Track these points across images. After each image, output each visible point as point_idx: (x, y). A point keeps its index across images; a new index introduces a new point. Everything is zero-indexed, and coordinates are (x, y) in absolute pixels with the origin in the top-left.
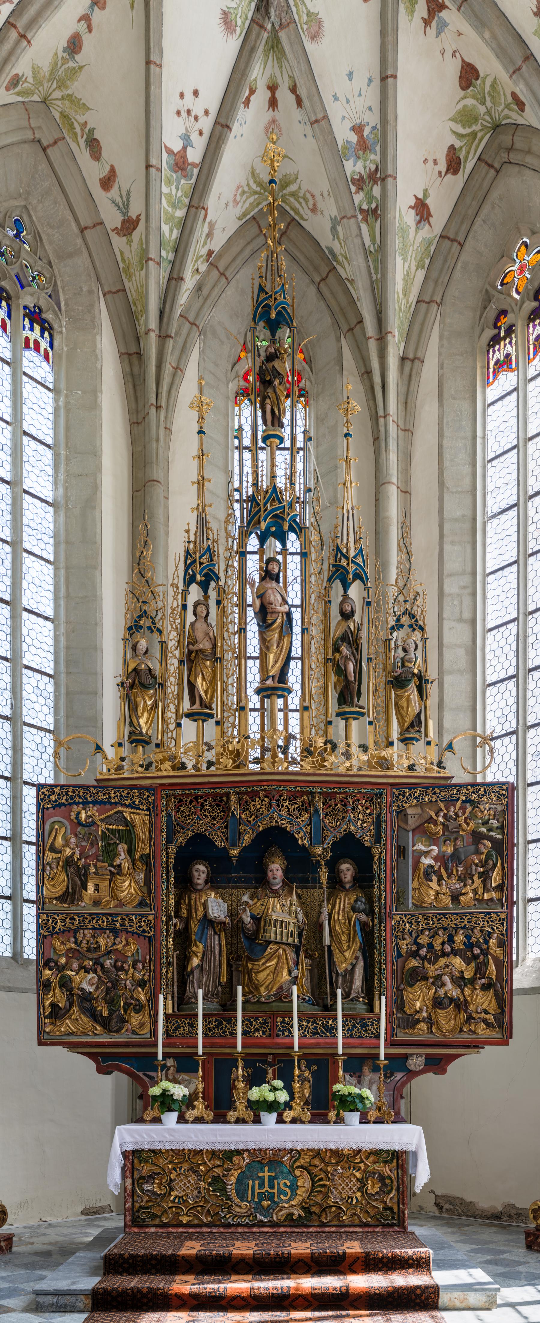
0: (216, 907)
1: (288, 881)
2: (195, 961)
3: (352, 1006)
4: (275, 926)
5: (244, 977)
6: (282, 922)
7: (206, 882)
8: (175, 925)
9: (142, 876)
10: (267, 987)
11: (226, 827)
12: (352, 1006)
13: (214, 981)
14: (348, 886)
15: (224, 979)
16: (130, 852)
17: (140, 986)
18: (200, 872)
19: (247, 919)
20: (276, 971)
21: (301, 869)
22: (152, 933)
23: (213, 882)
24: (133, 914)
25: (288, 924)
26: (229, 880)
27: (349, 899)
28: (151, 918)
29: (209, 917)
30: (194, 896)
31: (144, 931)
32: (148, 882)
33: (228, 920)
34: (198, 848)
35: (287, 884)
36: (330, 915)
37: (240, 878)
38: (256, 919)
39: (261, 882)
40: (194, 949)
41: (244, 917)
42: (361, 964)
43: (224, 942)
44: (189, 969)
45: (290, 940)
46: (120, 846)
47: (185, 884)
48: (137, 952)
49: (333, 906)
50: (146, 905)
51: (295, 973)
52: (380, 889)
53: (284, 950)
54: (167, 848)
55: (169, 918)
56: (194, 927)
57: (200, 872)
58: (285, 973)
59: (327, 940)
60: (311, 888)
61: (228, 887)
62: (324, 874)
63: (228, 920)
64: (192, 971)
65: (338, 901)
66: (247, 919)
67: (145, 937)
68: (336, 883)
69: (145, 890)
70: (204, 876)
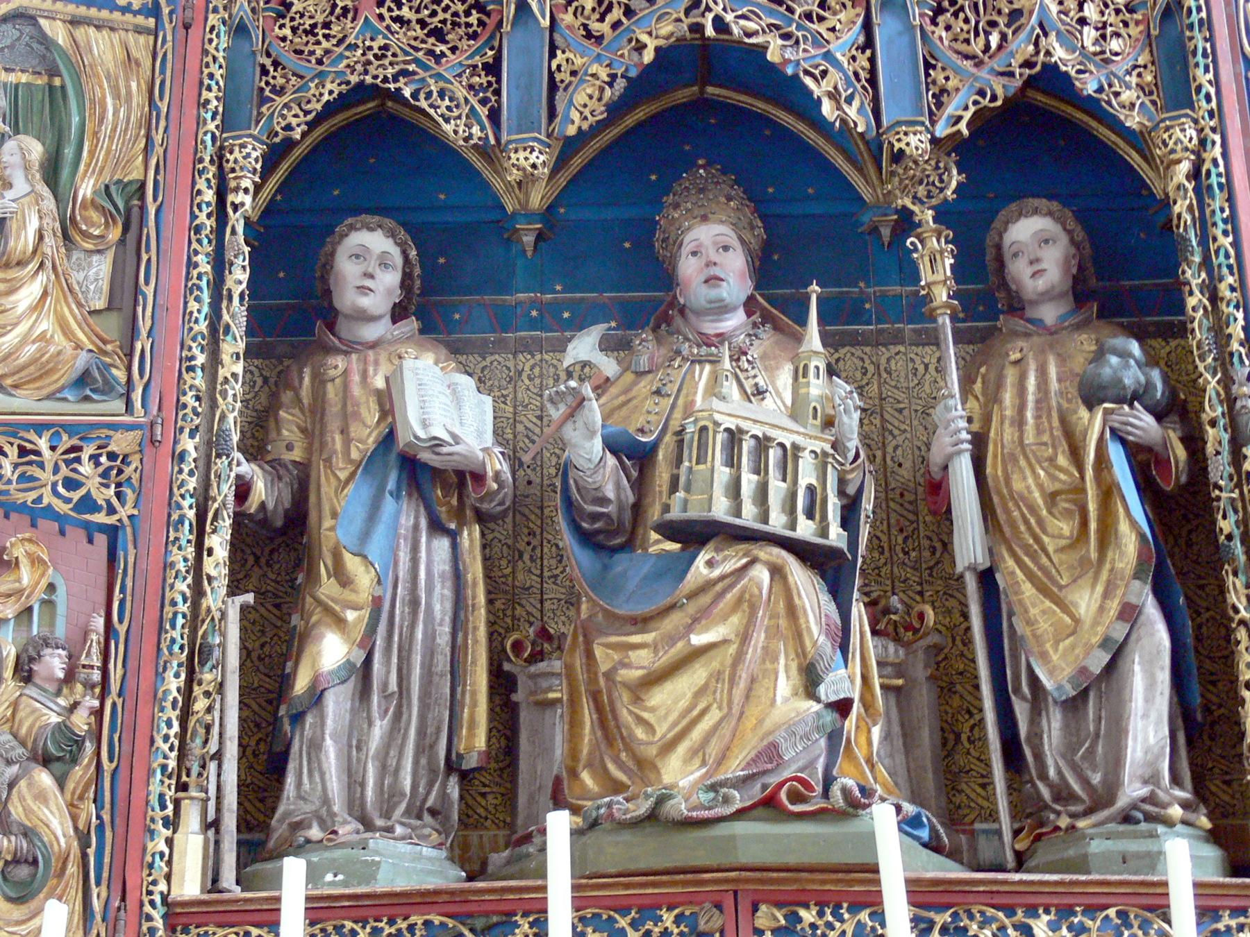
0: (446, 406)
1: (775, 302)
2: (331, 651)
3: (1133, 846)
4: (732, 461)
5: (574, 724)
6: (762, 444)
7: (398, 313)
8: (243, 490)
9: (102, 267)
10: (699, 750)
11: (493, 69)
12: (1133, 846)
13: (425, 747)
14: (1049, 314)
15: (477, 740)
16: (52, 171)
17: (46, 761)
18: (369, 264)
19: (588, 450)
20: (738, 684)
21: (824, 256)
22: (124, 512)
23: (427, 305)
24: (40, 428)
25: (791, 455)
26: (503, 320)
27: (1062, 359)
28: (121, 443)
29: (403, 438)
30: (339, 362)
31: (87, 504)
32: (124, 295)
33: (497, 464)
34: (366, 152)
35: (767, 318)
36: (979, 443)
37: (556, 307)
38: (635, 456)
39: (649, 304)
40: (327, 588)
41: (572, 433)
42: (1156, 634)
43: (475, 570)
44: (301, 684)
45: (805, 530)
46: (10, 145)
47: (295, 319)
48: (48, 604)
49: (993, 397)
50: (107, 388)
51: (840, 681)
52: (1214, 298)
53: (777, 572)
54: (219, 159)
55: (214, 446)
56: (342, 510)
57: (369, 264)
58: (785, 684)
59: (970, 544)
60: (878, 341)
61: (500, 346)
62: (937, 267)
63: (497, 464)
64: (316, 697)
65: (1011, 375)
66: (588, 450)
67: (90, 531)
68: (989, 300)
69: (112, 326)
70: (389, 281)
